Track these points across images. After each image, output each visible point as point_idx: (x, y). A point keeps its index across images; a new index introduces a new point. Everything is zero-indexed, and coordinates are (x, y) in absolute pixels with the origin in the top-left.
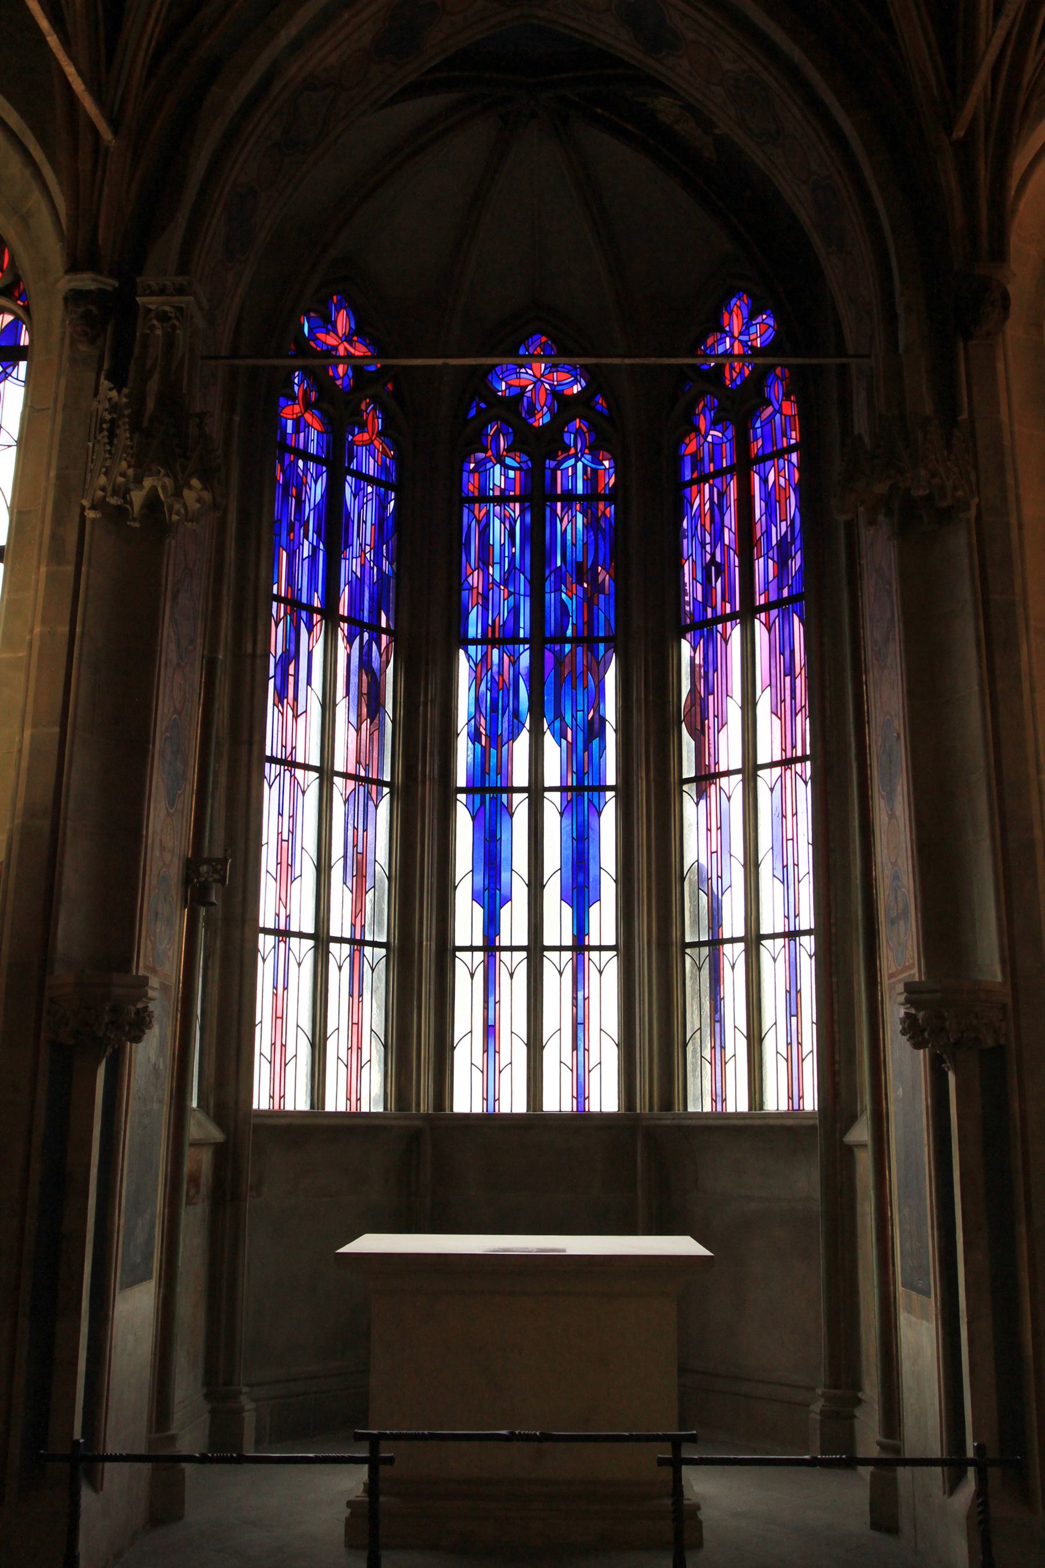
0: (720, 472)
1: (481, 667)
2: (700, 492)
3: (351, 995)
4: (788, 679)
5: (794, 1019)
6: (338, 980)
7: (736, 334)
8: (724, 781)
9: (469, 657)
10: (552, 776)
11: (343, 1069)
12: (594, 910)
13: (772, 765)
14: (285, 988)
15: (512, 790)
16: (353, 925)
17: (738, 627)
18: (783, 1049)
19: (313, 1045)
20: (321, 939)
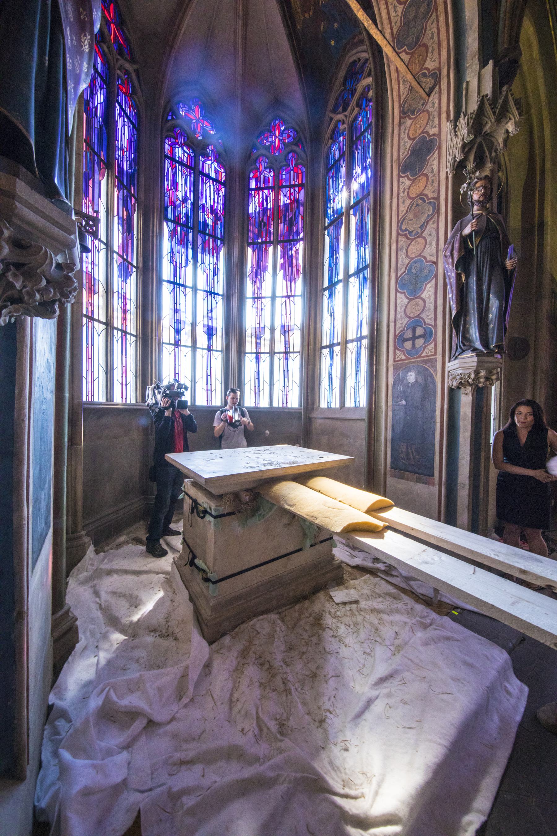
0: (268, 188)
1: (173, 233)
2: (259, 194)
3: (122, 354)
4: (290, 268)
5: (286, 379)
6: (117, 346)
7: (277, 135)
8: (263, 300)
9: (168, 226)
10: (201, 285)
11: (119, 385)
12: (214, 337)
13: (283, 297)
14: (92, 345)
15: (185, 286)
16: (123, 324)
17: (272, 247)
18: (281, 388)
19: (106, 373)
20: (109, 324)
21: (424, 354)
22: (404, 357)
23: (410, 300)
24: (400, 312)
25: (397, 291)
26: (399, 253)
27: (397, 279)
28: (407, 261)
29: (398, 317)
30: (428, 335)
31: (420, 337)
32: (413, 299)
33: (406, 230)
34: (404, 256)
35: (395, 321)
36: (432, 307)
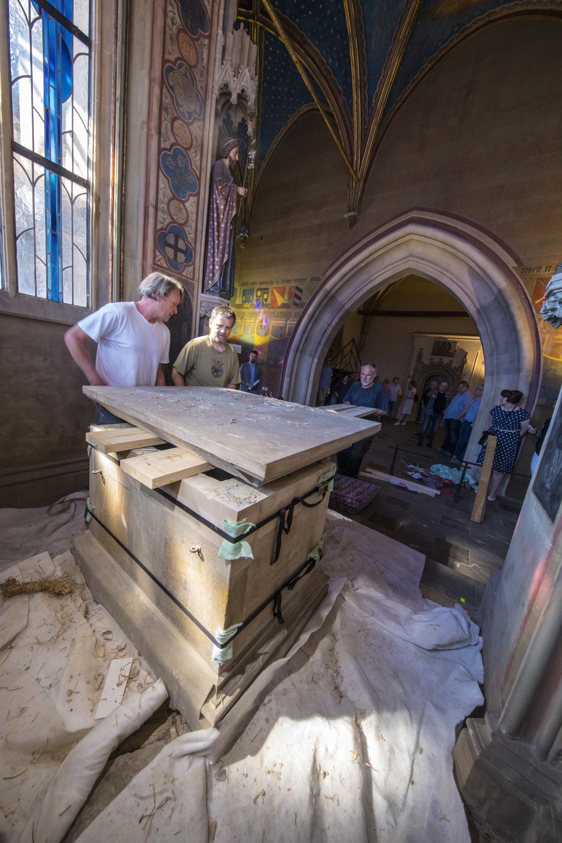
21: (184, 273)
22: (165, 265)
23: (174, 198)
24: (163, 203)
25: (159, 168)
26: (163, 112)
27: (160, 150)
28: (173, 140)
29: (161, 206)
30: (189, 254)
31: (181, 251)
32: (177, 199)
33: (172, 88)
34: (169, 125)
35: (156, 208)
36: (194, 227)
